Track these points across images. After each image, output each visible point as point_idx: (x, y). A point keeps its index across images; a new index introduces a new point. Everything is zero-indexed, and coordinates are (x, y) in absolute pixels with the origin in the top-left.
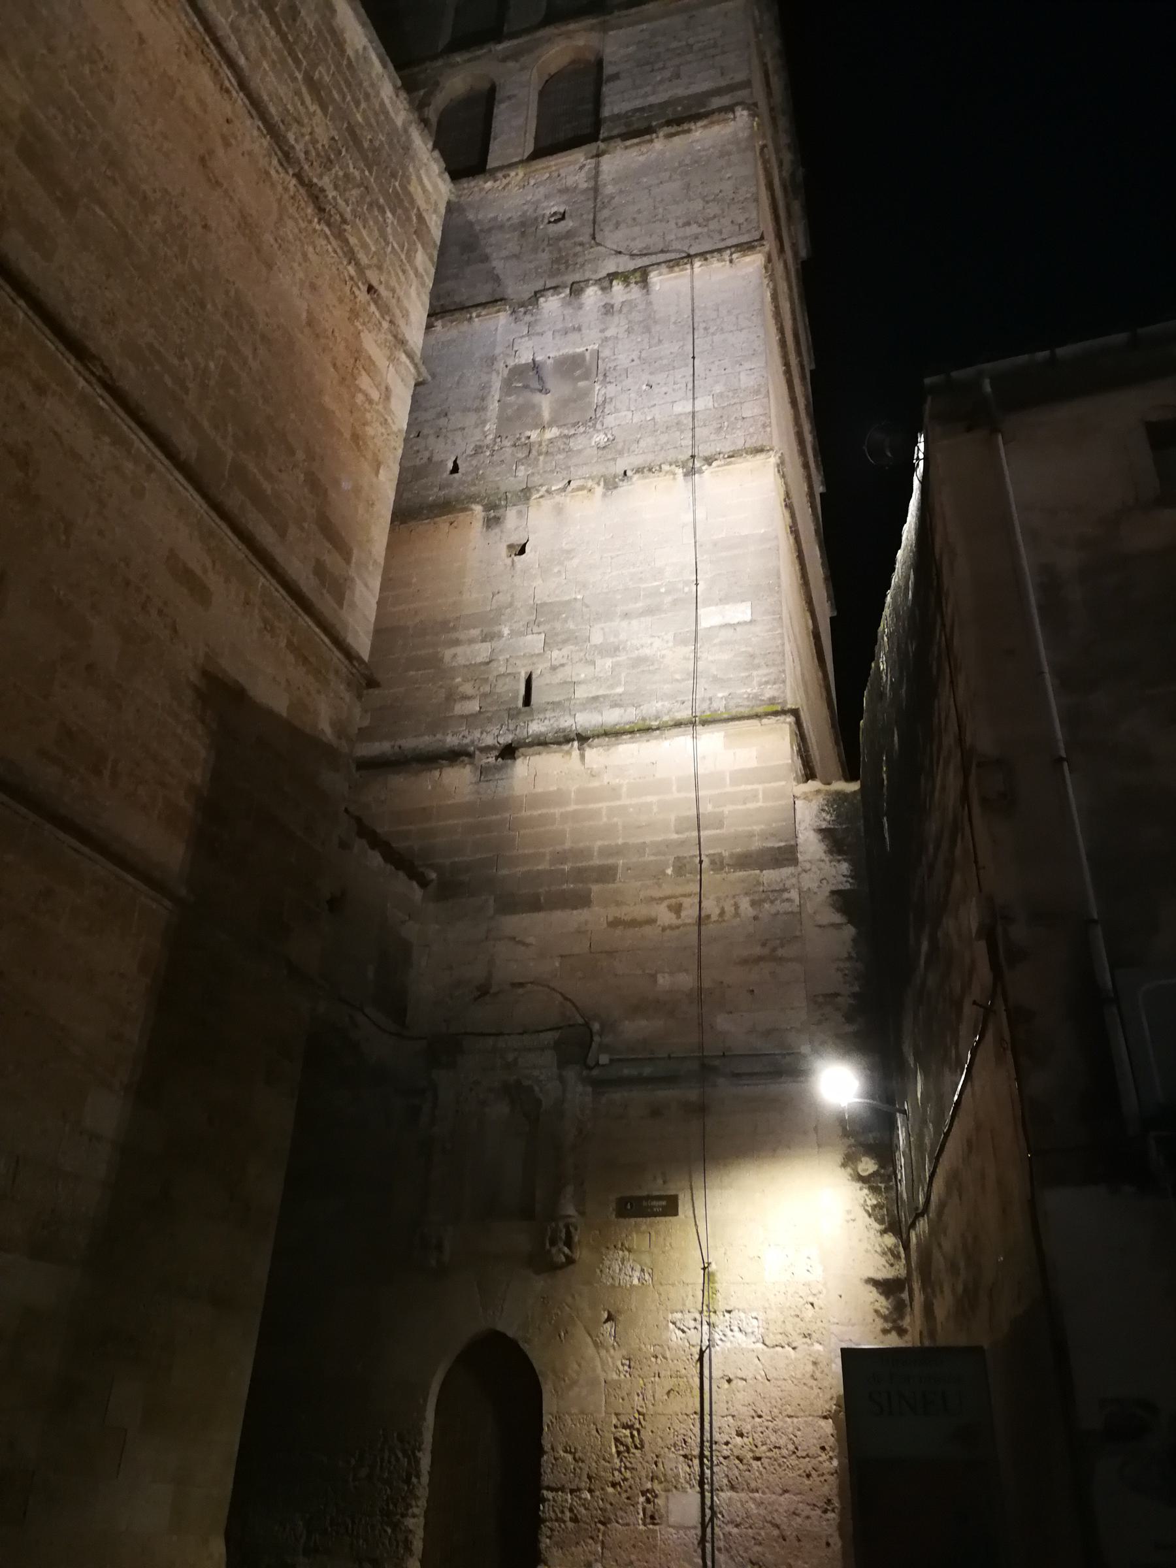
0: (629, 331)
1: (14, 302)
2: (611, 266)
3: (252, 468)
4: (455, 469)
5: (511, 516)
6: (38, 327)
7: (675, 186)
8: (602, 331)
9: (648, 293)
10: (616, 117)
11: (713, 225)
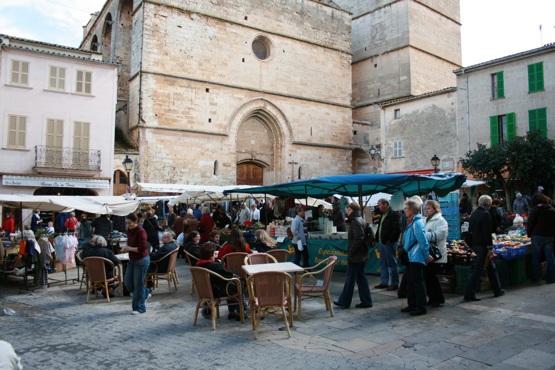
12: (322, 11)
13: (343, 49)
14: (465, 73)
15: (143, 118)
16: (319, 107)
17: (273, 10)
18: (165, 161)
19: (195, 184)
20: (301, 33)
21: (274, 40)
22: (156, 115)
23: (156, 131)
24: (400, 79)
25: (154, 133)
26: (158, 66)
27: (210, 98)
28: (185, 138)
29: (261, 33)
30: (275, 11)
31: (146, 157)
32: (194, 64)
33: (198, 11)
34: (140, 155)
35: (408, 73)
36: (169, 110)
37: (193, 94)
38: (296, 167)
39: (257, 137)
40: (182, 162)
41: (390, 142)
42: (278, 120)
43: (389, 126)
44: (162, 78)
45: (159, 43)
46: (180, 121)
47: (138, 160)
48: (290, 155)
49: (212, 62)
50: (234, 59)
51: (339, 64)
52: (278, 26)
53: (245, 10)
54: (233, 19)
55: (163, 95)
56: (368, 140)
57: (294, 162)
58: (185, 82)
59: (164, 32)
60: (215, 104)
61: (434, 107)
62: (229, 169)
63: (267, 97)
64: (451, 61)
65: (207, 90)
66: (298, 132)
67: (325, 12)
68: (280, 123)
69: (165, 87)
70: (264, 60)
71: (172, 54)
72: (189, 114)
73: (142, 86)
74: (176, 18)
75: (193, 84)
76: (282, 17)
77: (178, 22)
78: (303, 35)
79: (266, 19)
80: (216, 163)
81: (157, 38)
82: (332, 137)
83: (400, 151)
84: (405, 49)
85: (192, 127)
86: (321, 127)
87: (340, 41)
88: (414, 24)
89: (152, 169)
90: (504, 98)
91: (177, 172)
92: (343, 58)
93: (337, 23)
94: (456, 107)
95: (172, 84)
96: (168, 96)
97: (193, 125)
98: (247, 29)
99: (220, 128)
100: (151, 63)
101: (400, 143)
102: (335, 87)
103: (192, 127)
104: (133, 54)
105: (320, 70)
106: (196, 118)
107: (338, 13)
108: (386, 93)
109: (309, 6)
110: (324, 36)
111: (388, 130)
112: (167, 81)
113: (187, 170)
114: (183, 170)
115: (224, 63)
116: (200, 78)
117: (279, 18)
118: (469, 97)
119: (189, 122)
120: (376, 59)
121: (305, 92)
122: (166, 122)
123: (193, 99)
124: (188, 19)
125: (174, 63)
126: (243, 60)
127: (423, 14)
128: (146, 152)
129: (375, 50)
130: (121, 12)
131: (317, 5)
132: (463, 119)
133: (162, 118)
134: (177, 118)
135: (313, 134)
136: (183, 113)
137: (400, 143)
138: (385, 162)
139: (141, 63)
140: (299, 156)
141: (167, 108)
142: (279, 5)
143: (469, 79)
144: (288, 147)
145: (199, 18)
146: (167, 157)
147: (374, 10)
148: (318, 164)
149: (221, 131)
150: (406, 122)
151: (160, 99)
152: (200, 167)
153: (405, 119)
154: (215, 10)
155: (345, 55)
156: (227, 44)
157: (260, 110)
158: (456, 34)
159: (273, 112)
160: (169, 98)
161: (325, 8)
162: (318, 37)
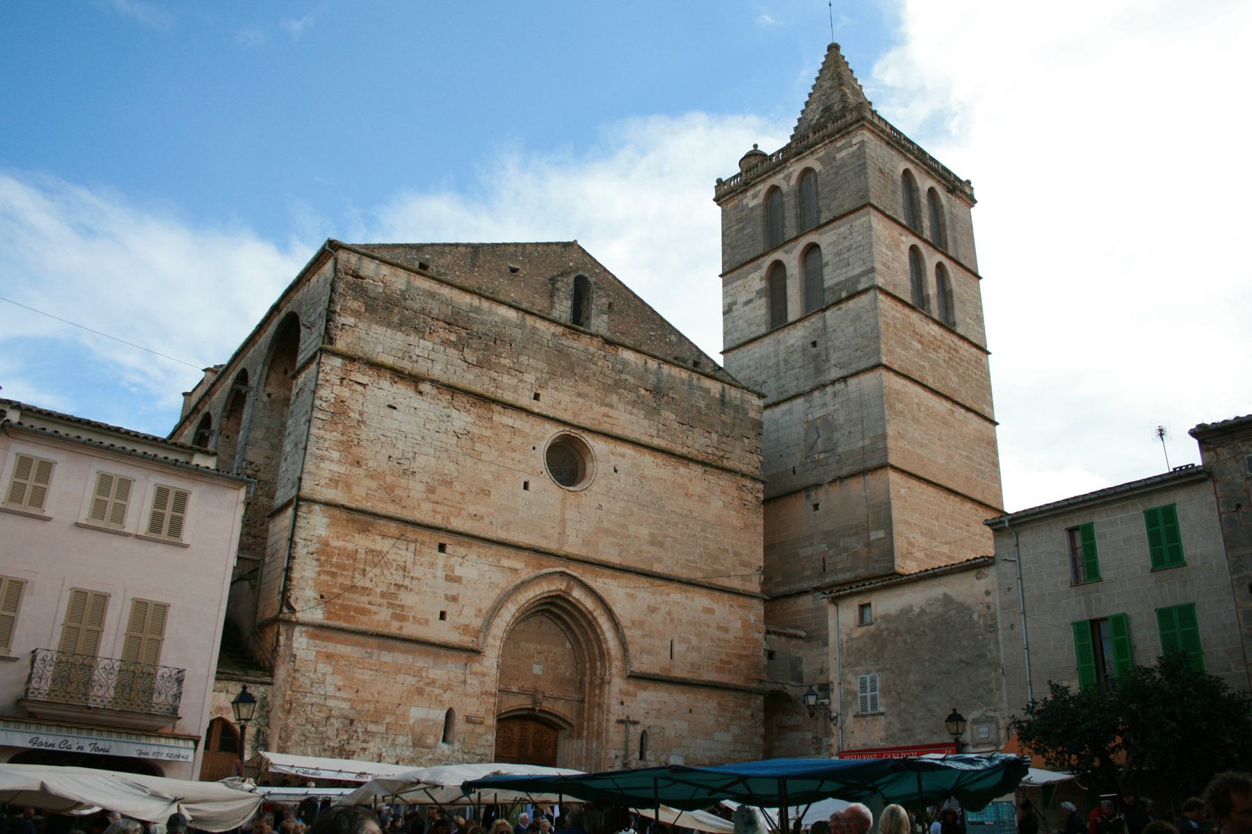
0: (842, 406)
2: (835, 373)
3: (717, 566)
4: (794, 472)
5: (813, 493)
7: (851, 329)
8: (834, 405)
9: (847, 387)
10: (830, 288)
11: (866, 350)
12: (701, 389)
13: (744, 468)
14: (1010, 525)
15: (292, 601)
16: (689, 595)
17: (595, 382)
18: (331, 703)
19: (397, 763)
20: (654, 433)
21: (597, 446)
22: (322, 597)
23: (318, 632)
24: (869, 537)
25: (312, 637)
26: (336, 488)
27: (445, 566)
28: (383, 652)
29: (567, 430)
30: (600, 384)
31: (290, 692)
32: (417, 489)
33: (435, 377)
34: (275, 686)
35: (887, 524)
36: (353, 588)
37: (410, 555)
38: (636, 732)
39: (546, 659)
40: (372, 707)
41: (850, 677)
42: (597, 622)
43: (847, 642)
44: (344, 515)
45: (345, 438)
46: (375, 613)
47: (269, 699)
48: (622, 703)
49: (457, 486)
50: (505, 482)
51: (736, 502)
52: (605, 415)
53: (537, 379)
54: (508, 397)
55: (343, 552)
56: (801, 673)
57: (631, 719)
58: (393, 528)
59: (357, 416)
60: (458, 580)
61: (947, 600)
62: (480, 729)
63: (574, 570)
64: (979, 498)
65: (442, 548)
66: (642, 651)
67: (708, 391)
68: (601, 628)
69: (347, 535)
70: (571, 488)
71: (370, 465)
72: (396, 598)
73: (297, 530)
74: (387, 390)
75: (411, 533)
76: (614, 398)
77: (390, 398)
78: (658, 437)
79: (580, 400)
80: (450, 715)
81: (340, 428)
82: (719, 664)
83: (874, 699)
84: (879, 473)
85: (401, 628)
86: (694, 641)
87: (738, 451)
88: (895, 421)
89: (299, 721)
90: (1101, 580)
91: (356, 732)
92: (744, 489)
93: (732, 414)
94: (995, 599)
95: (364, 530)
96: (353, 556)
97: (404, 624)
98: (538, 420)
99: (464, 635)
100: (323, 482)
101: (873, 681)
102: (727, 551)
103: (401, 628)
104: (286, 459)
105: (695, 514)
106: (412, 608)
107: (734, 393)
108: (840, 566)
109: (674, 378)
110: (703, 441)
111: (845, 651)
112: (354, 521)
113: (382, 729)
114: (372, 727)
115: (483, 490)
116: (427, 519)
117: (608, 400)
118: (1023, 577)
119: (395, 617)
120: (816, 493)
121: (659, 560)
122: (343, 613)
123: (409, 565)
124: (411, 393)
125: (374, 484)
126: (526, 486)
127: (916, 400)
128: (290, 679)
129: (814, 473)
130: (269, 369)
131: (690, 375)
132: (1012, 627)
133: (335, 604)
134: (369, 607)
135: (676, 656)
136: (383, 595)
137: (873, 681)
138: (839, 724)
139: (300, 479)
140: (643, 705)
141: (349, 583)
142: (608, 372)
143: (1020, 540)
144: (617, 684)
145: (435, 392)
146: (338, 694)
147: (812, 390)
148: (685, 725)
149: (467, 641)
150: (885, 633)
151: (334, 560)
152: (411, 722)
153: (883, 627)
154: (471, 377)
155: (749, 483)
156: (493, 450)
157: (558, 596)
158: (988, 443)
159: (588, 603)
160: (355, 560)
161: (707, 383)
162: (690, 442)
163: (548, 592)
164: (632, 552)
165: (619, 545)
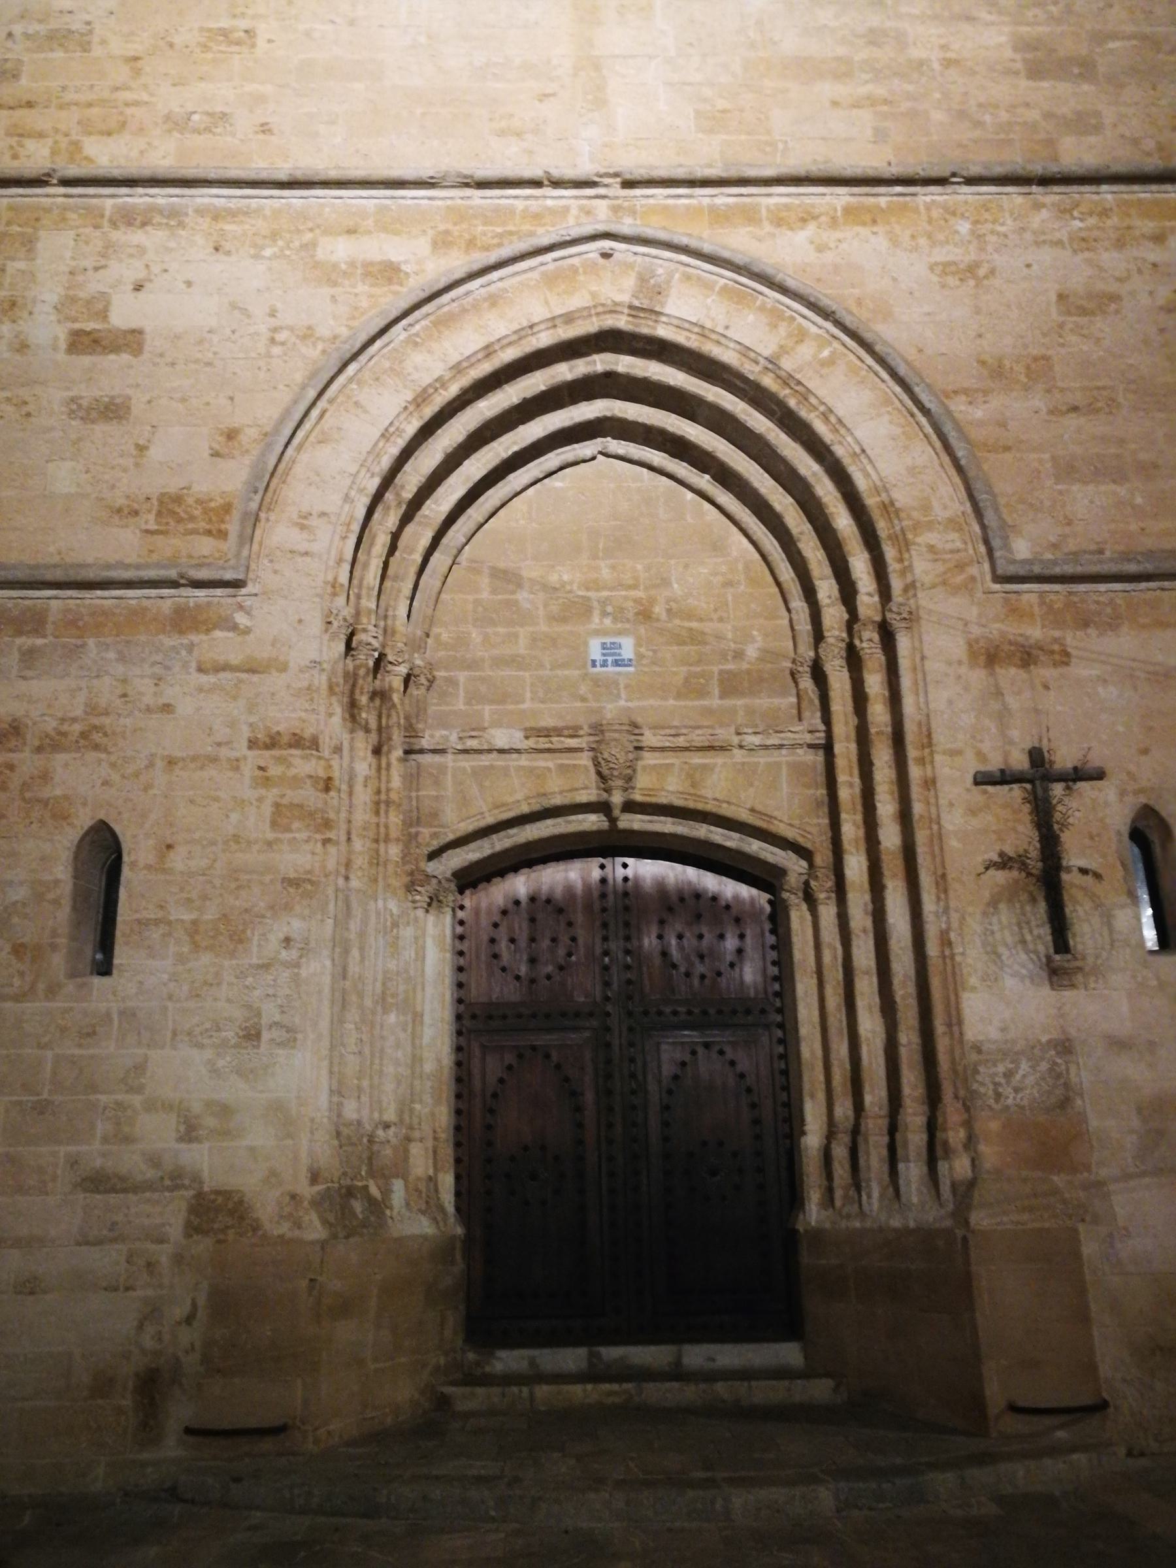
1: (1098, 193)
6: (1127, 193)
42: (805, 395)
163: (552, 322)
164: (938, 116)
165: (872, 101)
